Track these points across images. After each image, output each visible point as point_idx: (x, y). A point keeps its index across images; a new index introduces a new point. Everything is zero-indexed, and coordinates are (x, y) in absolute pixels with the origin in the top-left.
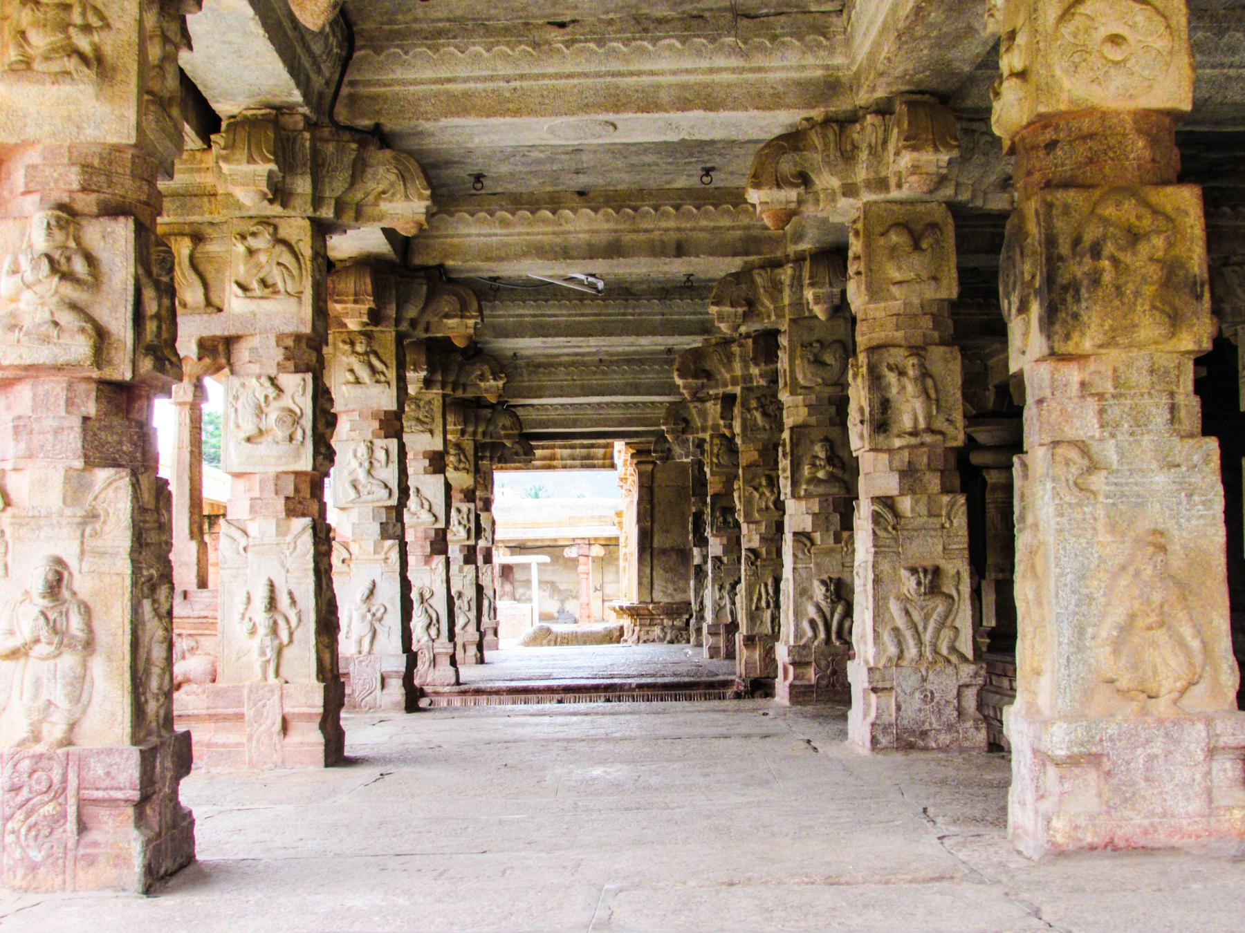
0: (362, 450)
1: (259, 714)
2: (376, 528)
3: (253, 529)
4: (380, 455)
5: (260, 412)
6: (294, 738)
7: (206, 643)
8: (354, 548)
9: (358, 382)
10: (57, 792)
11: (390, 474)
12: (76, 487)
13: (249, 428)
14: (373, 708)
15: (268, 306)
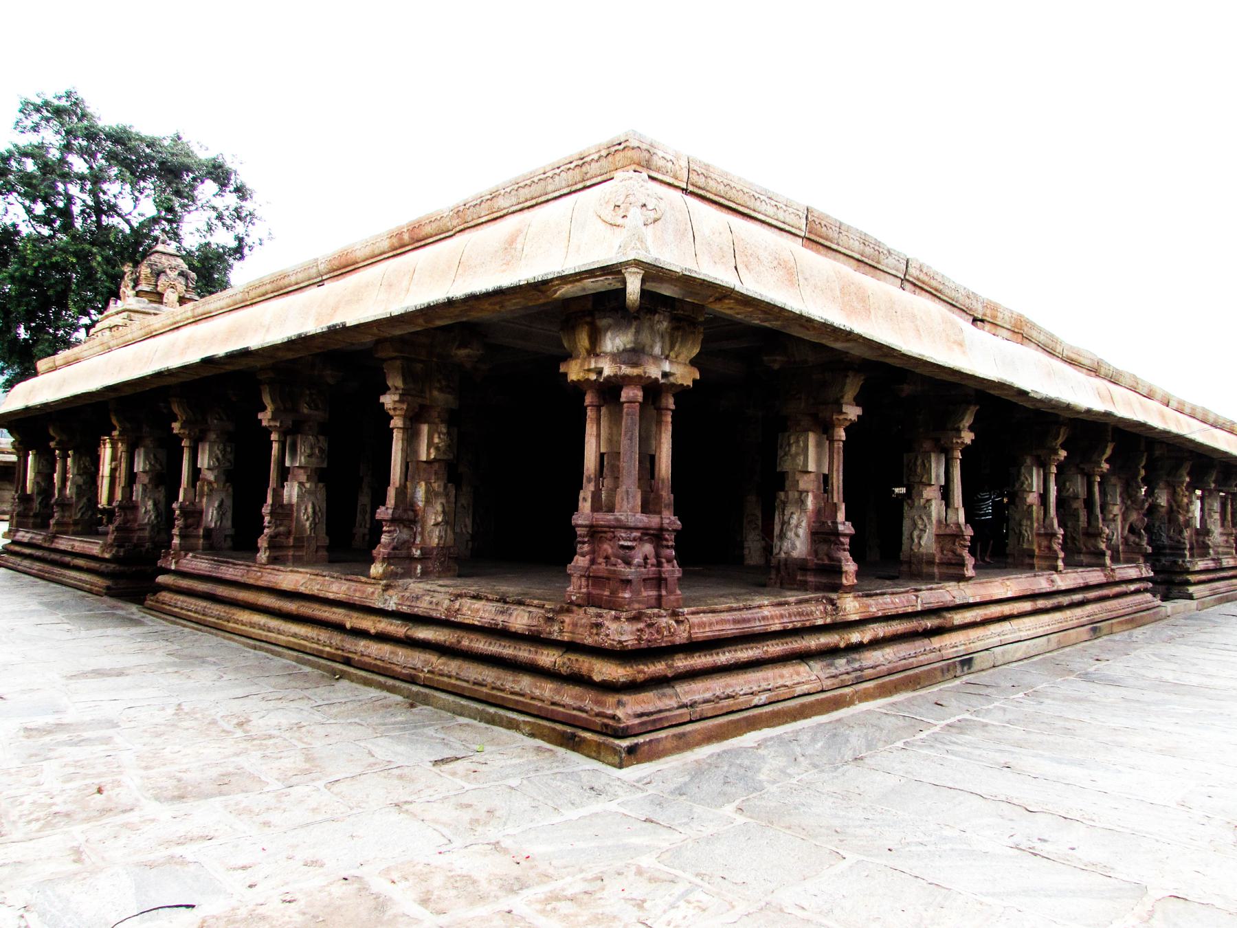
0: (221, 447)
1: (308, 547)
2: (223, 478)
3: (308, 485)
4: (229, 449)
5: (312, 448)
6: (320, 553)
7: (286, 522)
8: (215, 486)
9: (221, 419)
10: (444, 555)
11: (230, 457)
12: (445, 487)
13: (308, 451)
14: (221, 549)
15: (316, 413)
